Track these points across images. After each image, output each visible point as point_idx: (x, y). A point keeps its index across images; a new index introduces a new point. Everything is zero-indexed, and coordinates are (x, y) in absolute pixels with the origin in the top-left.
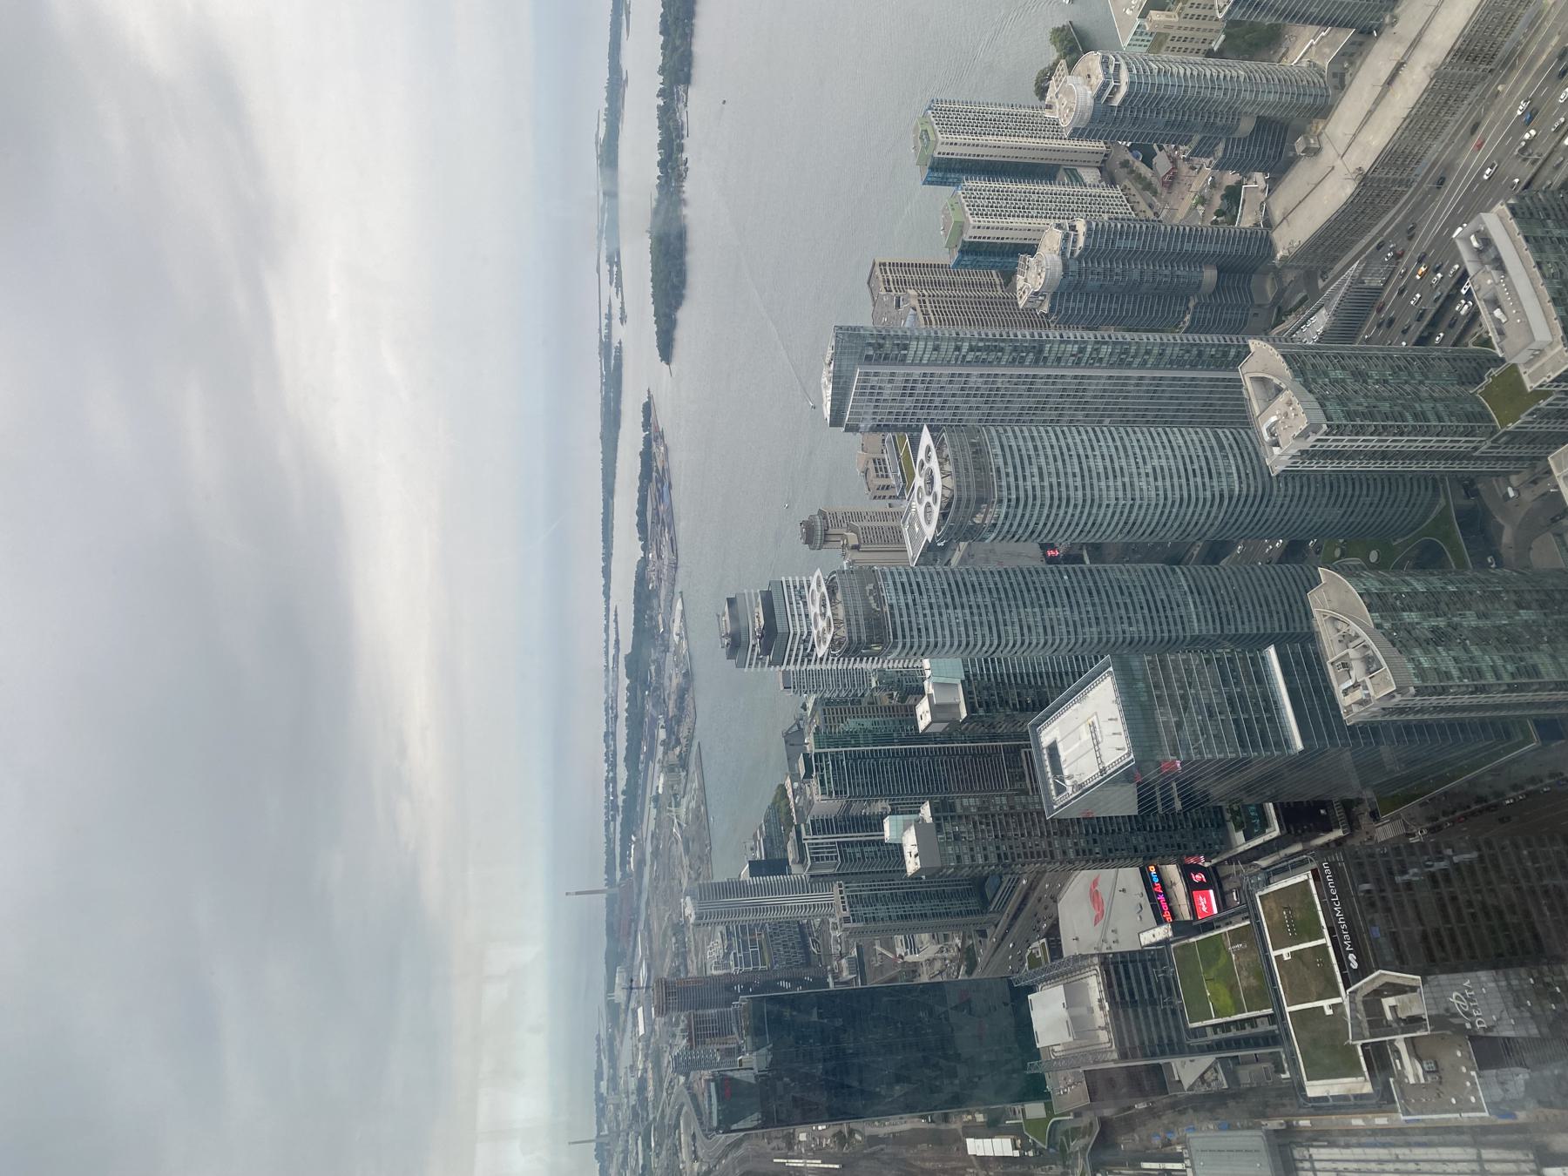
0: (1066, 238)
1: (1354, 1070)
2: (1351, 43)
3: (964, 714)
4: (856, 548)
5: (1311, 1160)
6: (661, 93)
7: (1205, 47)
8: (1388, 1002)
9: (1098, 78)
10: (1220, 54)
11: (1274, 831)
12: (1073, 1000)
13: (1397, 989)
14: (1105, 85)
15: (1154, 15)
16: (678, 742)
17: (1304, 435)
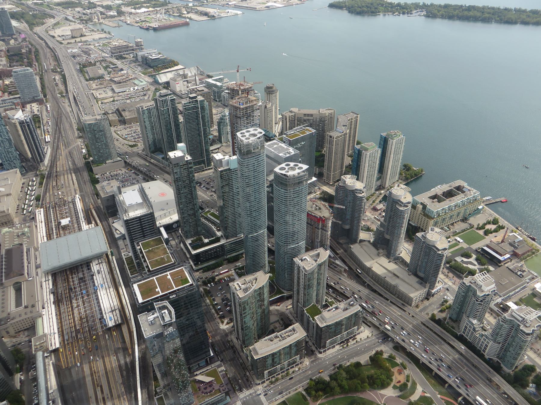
0: (361, 191)
1: (143, 299)
2: (406, 262)
3: (220, 170)
4: (266, 107)
5: (102, 263)
6: (424, 4)
7: (411, 219)
8: (166, 311)
9: (404, 201)
10: (408, 223)
11: (194, 252)
12: (139, 205)
13: (170, 313)
14: (402, 203)
15: (421, 207)
16: (188, 13)
17: (304, 268)
